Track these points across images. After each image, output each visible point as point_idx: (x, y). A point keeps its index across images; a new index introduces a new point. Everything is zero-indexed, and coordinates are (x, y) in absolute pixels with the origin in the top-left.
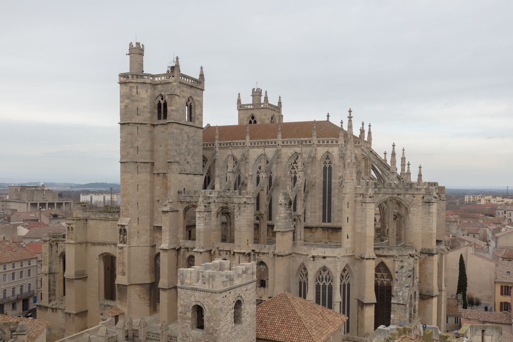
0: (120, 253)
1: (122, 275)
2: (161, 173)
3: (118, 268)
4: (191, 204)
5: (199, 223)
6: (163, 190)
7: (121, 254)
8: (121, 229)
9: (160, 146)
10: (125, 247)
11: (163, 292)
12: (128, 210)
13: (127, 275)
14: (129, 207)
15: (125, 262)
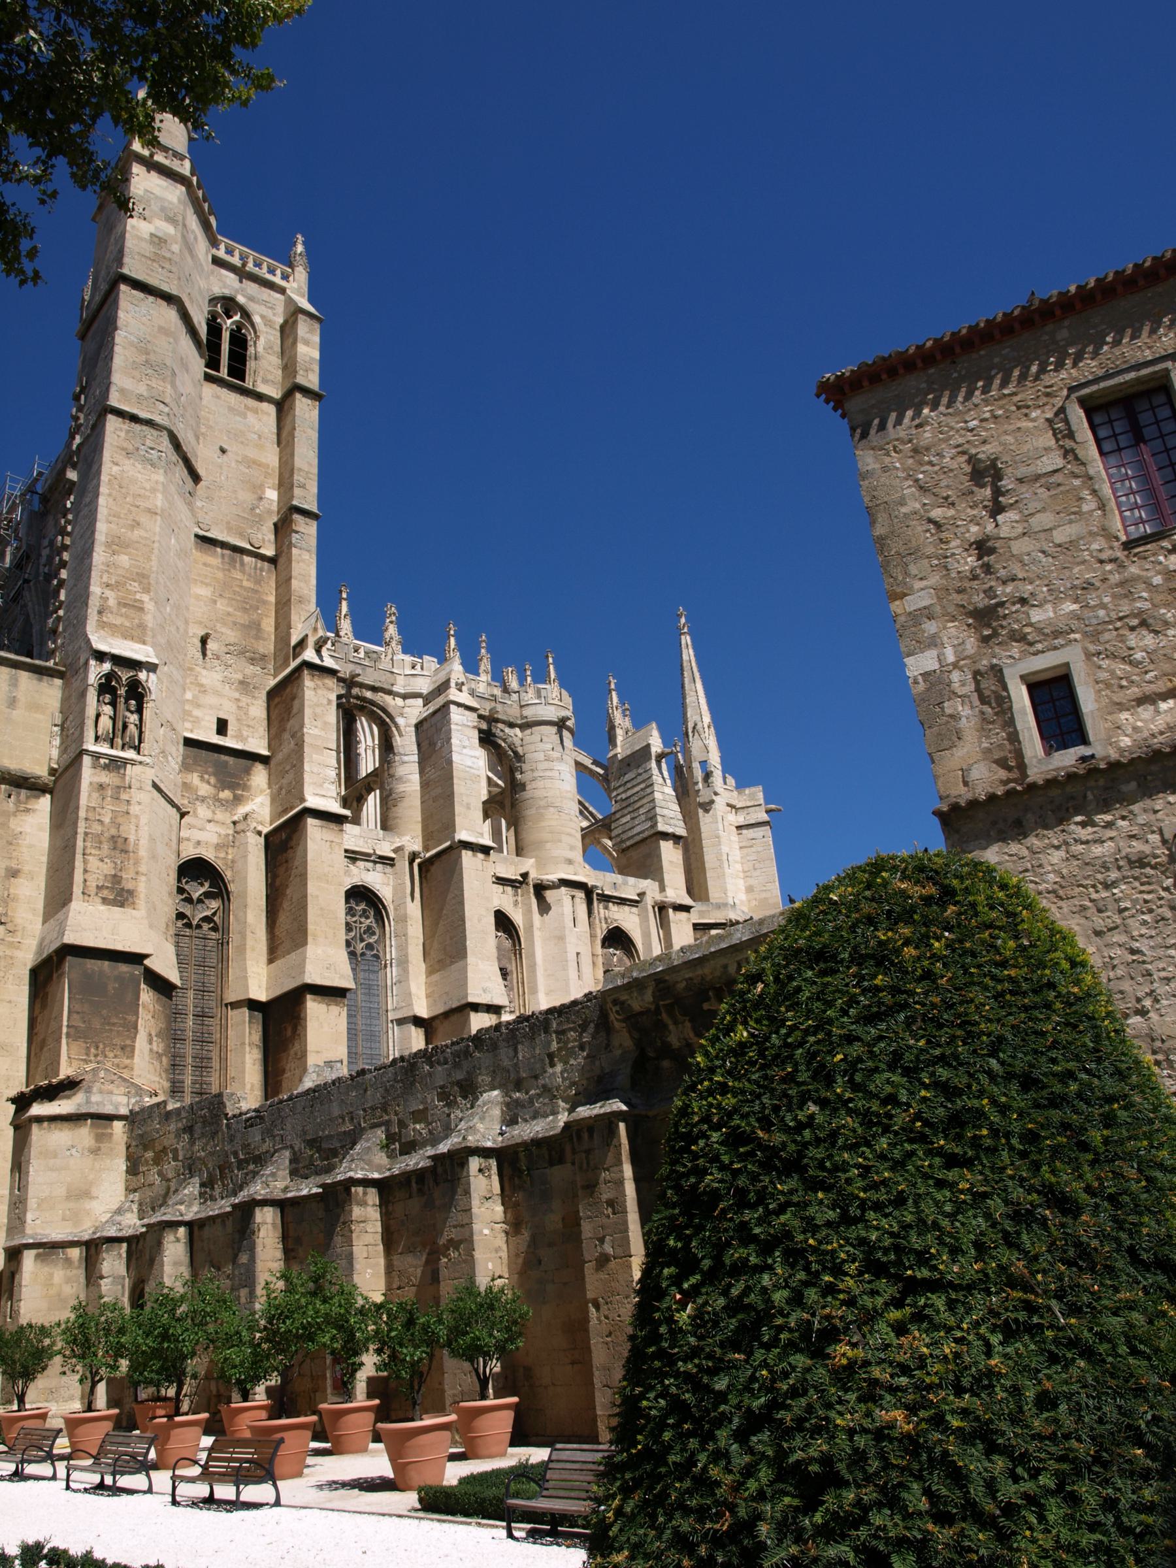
0: (101, 787)
1: (105, 901)
2: (224, 545)
3: (85, 862)
4: (355, 691)
5: (464, 747)
6: (230, 610)
7: (109, 793)
8: (109, 676)
9: (223, 451)
10: (133, 762)
11: (323, 1007)
12: (142, 609)
13: (141, 901)
14: (145, 598)
15: (132, 838)
